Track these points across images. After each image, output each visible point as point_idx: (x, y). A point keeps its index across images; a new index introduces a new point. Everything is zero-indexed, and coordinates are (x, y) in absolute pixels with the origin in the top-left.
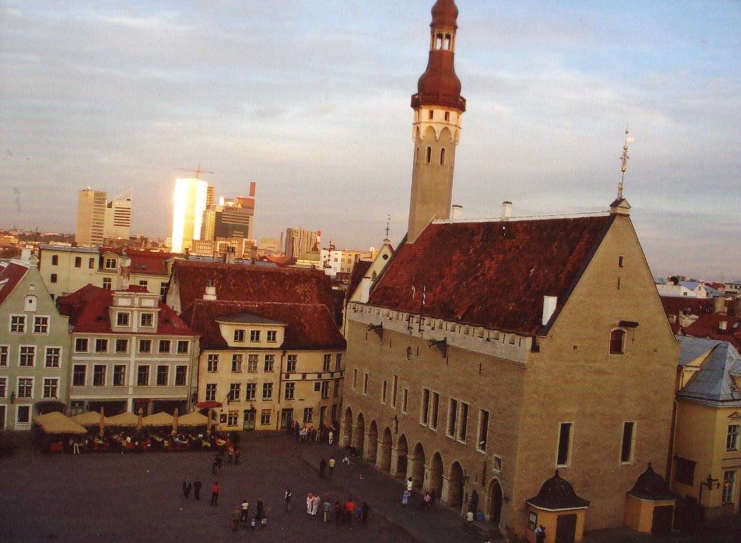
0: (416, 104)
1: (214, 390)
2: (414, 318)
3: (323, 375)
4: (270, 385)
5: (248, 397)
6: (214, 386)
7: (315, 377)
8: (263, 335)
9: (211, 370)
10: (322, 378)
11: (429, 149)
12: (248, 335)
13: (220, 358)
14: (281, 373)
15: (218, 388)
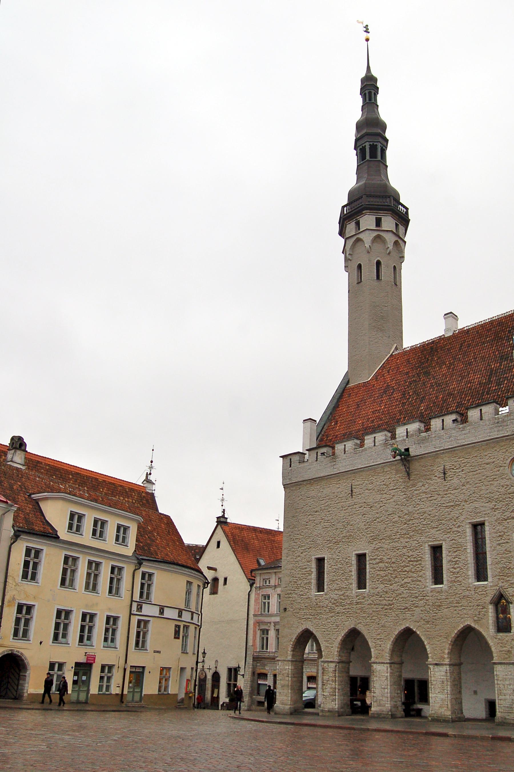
0: (349, 216)
1: (28, 617)
4: (116, 619)
5: (81, 639)
6: (29, 608)
8: (111, 531)
9: (27, 578)
11: (378, 263)
12: (88, 525)
13: (43, 556)
14: (132, 601)
15: (35, 613)
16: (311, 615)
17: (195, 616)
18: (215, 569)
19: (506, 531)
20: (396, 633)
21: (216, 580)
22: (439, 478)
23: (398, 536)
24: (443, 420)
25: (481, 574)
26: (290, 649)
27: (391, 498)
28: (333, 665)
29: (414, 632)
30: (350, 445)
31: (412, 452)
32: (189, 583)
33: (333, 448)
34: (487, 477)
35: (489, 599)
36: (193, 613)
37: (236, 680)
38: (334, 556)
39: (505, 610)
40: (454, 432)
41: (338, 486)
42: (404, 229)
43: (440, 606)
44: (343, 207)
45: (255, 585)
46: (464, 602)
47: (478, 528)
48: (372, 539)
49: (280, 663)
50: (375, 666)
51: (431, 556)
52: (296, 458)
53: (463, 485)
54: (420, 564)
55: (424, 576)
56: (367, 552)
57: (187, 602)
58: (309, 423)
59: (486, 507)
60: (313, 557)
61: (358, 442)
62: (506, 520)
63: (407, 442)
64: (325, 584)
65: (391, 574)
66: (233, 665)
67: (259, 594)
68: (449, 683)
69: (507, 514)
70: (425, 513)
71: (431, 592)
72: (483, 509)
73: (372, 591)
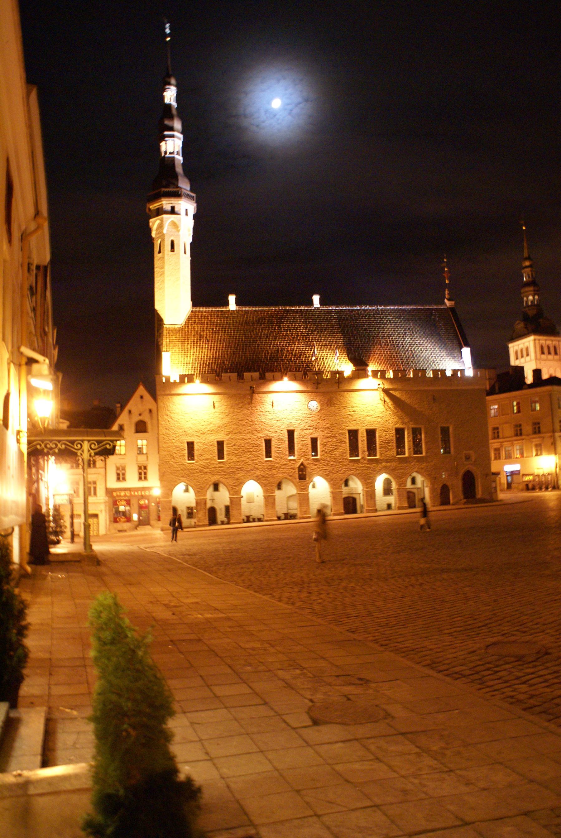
38: (202, 441)
46: (284, 466)
60: (185, 441)
69: (306, 427)
70: (262, 422)
73: (230, 461)
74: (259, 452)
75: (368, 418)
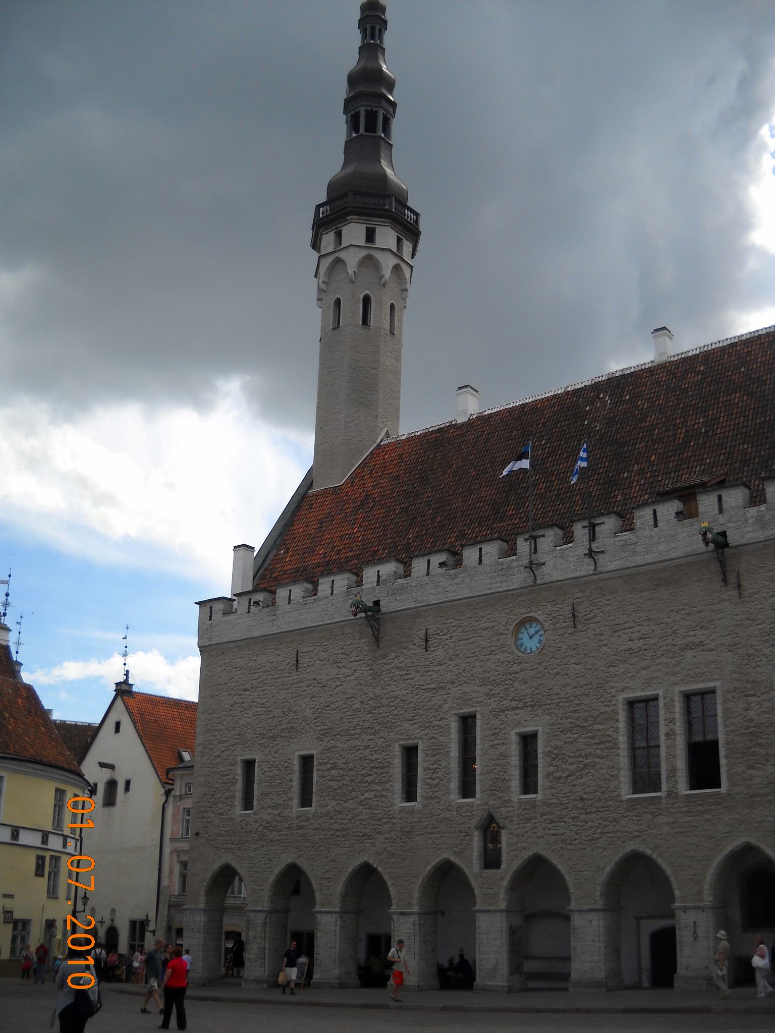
0: (327, 221)
2: (539, 540)
3: (51, 837)
7: (34, 840)
10: (51, 845)
11: (367, 300)
16: (233, 843)
17: (71, 844)
18: (111, 767)
19: (502, 727)
20: (350, 870)
21: (112, 785)
22: (419, 646)
23: (359, 731)
24: (429, 561)
25: (467, 789)
26: (202, 892)
27: (353, 674)
28: (262, 916)
29: (375, 870)
30: (298, 591)
31: (385, 607)
32: (60, 793)
33: (274, 593)
34: (483, 648)
35: (474, 823)
36: (65, 838)
37: (142, 938)
39: (496, 839)
40: (442, 579)
41: (277, 652)
42: (410, 245)
43: (410, 832)
44: (318, 207)
45: (173, 793)
47: (467, 723)
48: (324, 734)
49: (188, 913)
50: (319, 916)
51: (402, 760)
52: (219, 607)
53: (451, 659)
54: (387, 772)
55: (391, 789)
56: (315, 752)
57: (58, 820)
58: (242, 552)
59: (478, 692)
60: (239, 759)
61: (310, 586)
62: (504, 711)
63: (377, 591)
64: (255, 798)
65: (347, 786)
66: (139, 915)
67: (179, 807)
68: (417, 939)
70: (397, 697)
71: (400, 812)
72: (474, 695)
74: (387, 786)
75: (689, 654)
